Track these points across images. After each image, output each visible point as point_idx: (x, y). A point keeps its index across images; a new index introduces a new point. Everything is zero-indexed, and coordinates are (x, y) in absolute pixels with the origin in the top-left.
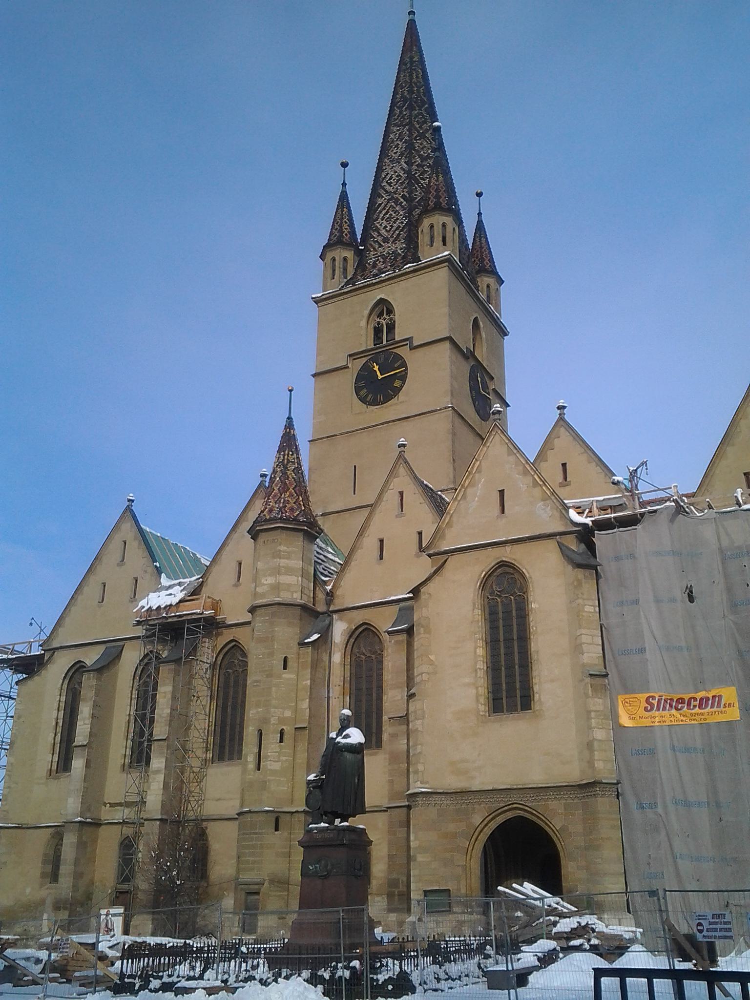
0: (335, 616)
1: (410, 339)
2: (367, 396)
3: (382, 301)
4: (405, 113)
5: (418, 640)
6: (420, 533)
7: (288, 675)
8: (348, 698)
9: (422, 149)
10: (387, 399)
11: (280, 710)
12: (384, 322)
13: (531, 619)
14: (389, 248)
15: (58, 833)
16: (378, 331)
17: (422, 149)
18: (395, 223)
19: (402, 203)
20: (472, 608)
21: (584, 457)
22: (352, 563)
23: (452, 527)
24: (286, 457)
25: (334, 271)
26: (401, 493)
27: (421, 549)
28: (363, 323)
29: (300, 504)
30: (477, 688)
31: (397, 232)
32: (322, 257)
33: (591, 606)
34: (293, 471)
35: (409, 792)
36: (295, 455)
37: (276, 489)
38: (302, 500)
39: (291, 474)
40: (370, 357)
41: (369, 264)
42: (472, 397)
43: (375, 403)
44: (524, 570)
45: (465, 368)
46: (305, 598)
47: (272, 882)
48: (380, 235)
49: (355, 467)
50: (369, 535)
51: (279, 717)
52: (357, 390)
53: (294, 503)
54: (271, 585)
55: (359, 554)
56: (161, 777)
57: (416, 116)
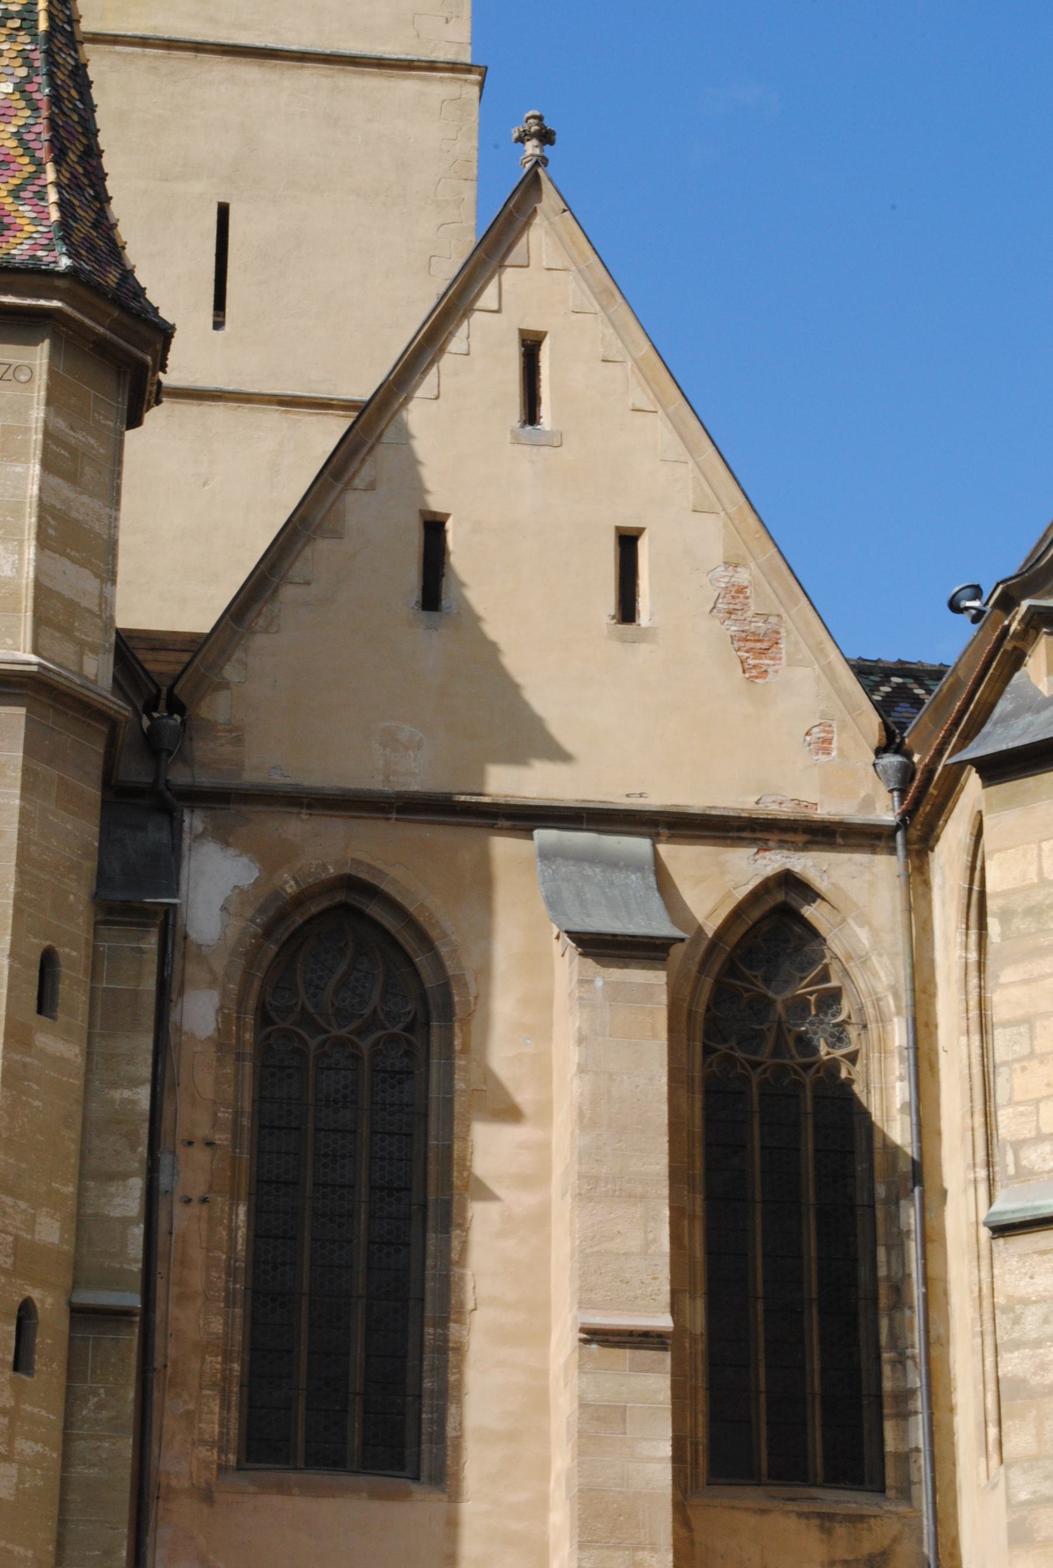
8: (242, 1210)
11: (23, 1205)
22: (288, 593)
50: (371, 487)
51: (17, 1237)
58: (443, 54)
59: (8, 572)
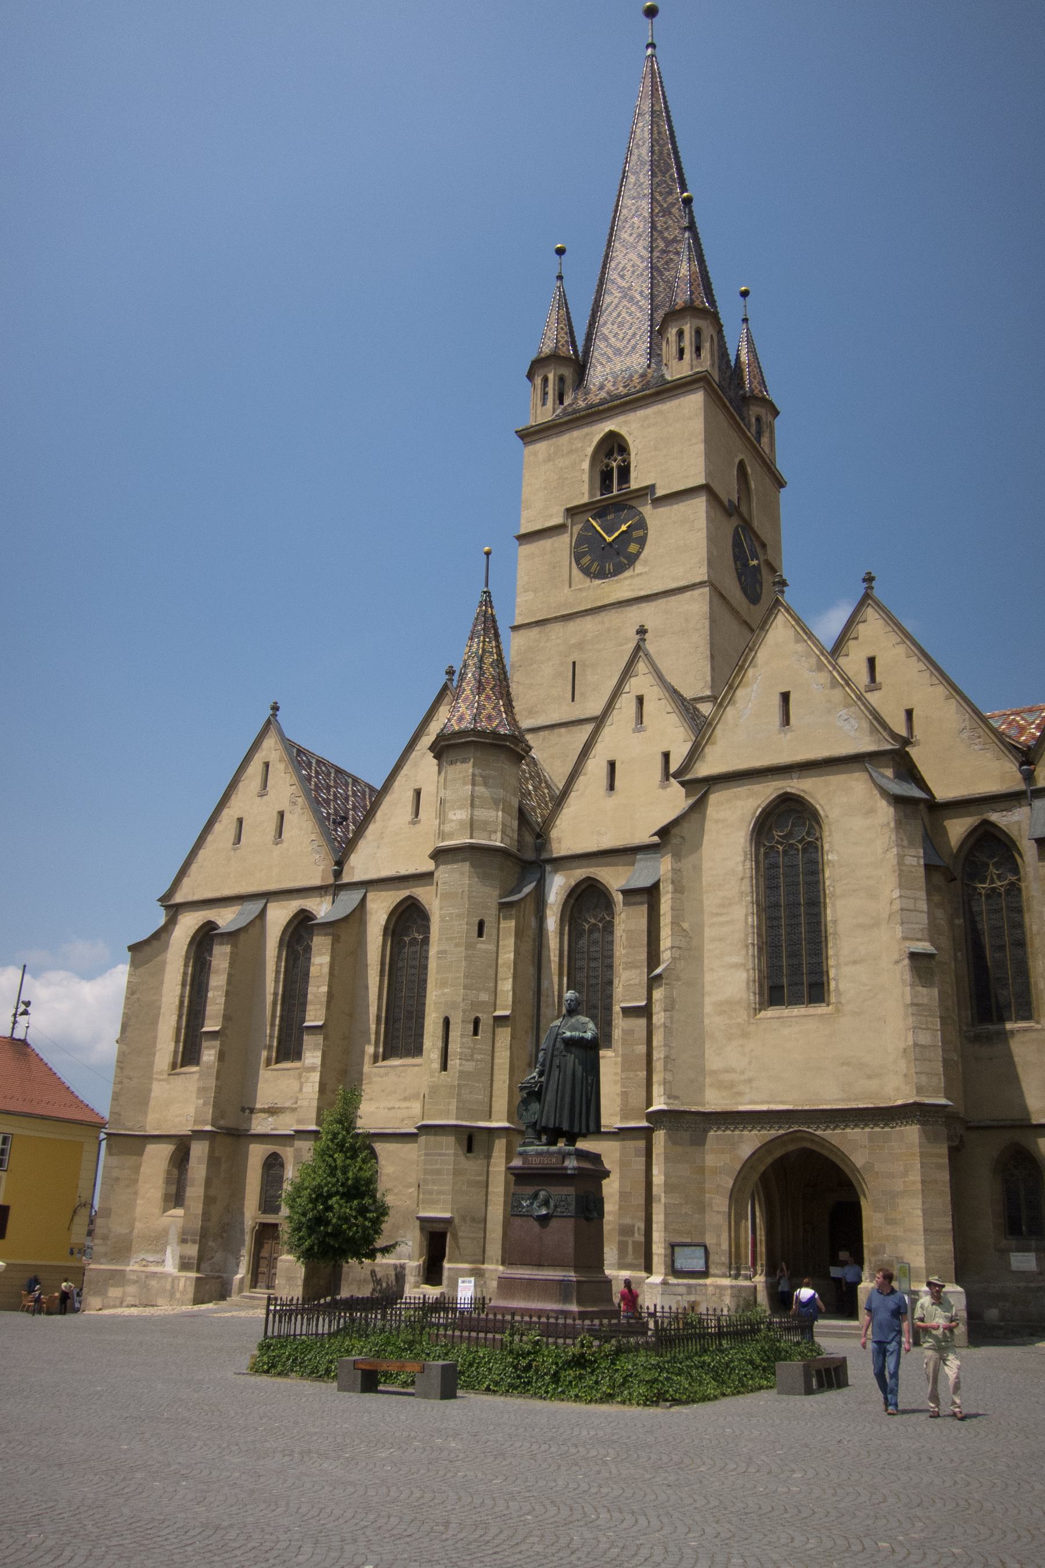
0: (548, 868)
1: (652, 488)
3: (612, 436)
4: (642, 181)
5: (665, 902)
6: (666, 756)
7: (485, 945)
9: (667, 229)
10: (619, 569)
12: (614, 464)
13: (827, 874)
14: (618, 365)
15: (182, 1147)
16: (606, 478)
17: (667, 229)
18: (630, 328)
19: (638, 302)
20: (742, 858)
21: (901, 650)
22: (573, 794)
23: (714, 743)
24: (481, 645)
25: (545, 394)
26: (640, 700)
27: (667, 775)
28: (586, 465)
29: (500, 711)
30: (748, 971)
31: (633, 342)
32: (530, 376)
33: (914, 857)
34: (492, 663)
35: (651, 1109)
36: (494, 642)
37: (468, 688)
38: (503, 705)
39: (488, 669)
40: (595, 511)
41: (594, 385)
42: (737, 569)
43: (601, 575)
44: (817, 806)
45: (729, 526)
46: (507, 840)
47: (463, 1219)
48: (610, 346)
49: (574, 663)
50: (594, 757)
52: (578, 557)
53: (493, 709)
54: (461, 822)
55: (581, 781)
56: (316, 1077)
57: (658, 185)
58: (698, 580)
59: (464, 817)
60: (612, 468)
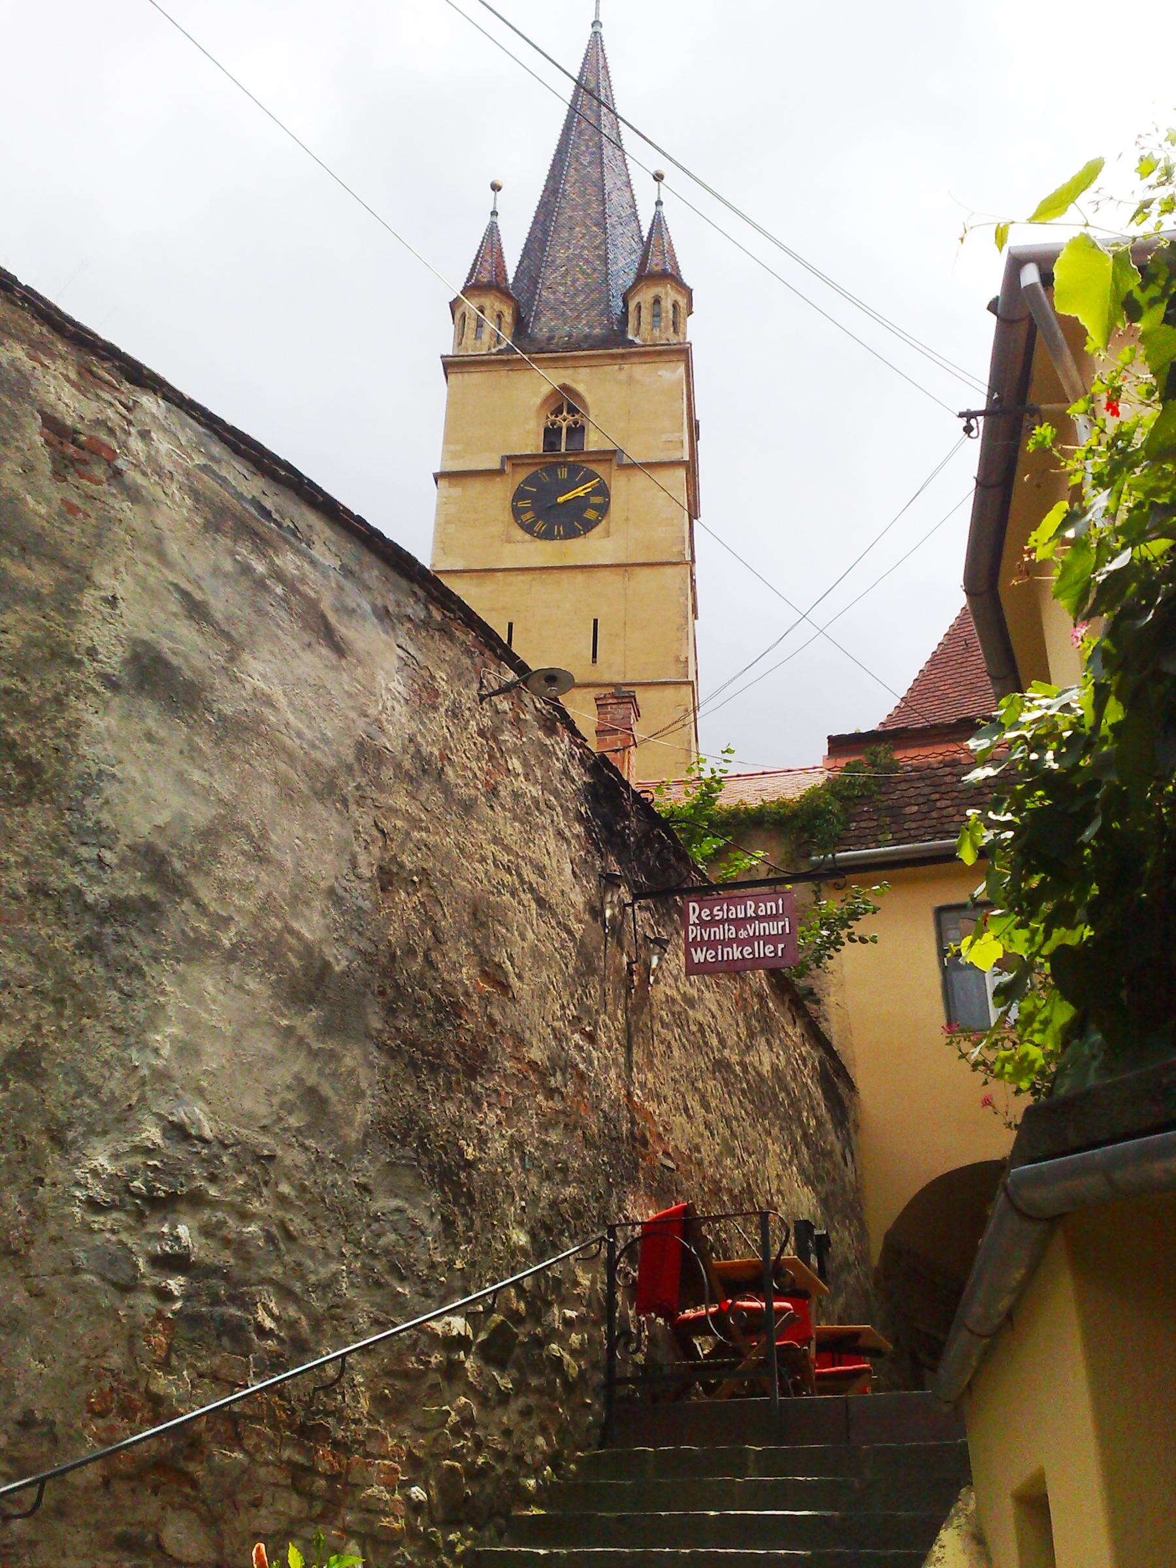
2: (534, 523)
10: (571, 534)
12: (564, 424)
16: (551, 435)
43: (548, 536)
52: (517, 513)
60: (560, 429)
